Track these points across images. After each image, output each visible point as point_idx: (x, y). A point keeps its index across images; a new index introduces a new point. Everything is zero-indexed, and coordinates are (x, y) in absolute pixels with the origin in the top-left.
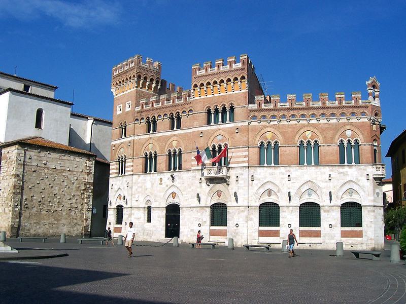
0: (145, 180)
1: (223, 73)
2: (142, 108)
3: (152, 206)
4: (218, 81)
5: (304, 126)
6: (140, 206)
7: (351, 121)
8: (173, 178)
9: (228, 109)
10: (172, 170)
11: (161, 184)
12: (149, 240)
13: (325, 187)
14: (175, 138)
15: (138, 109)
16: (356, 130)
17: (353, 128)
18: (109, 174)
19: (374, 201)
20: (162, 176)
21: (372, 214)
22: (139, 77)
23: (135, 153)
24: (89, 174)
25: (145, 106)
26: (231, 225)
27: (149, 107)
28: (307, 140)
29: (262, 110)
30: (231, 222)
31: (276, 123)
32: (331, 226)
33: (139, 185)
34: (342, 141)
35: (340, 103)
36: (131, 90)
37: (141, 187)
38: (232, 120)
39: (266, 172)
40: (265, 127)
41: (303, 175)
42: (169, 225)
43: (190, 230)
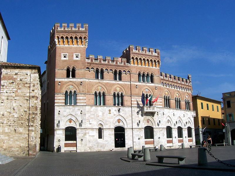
0: (97, 110)
1: (148, 55)
6: (94, 128)
8: (119, 111)
11: (110, 113)
12: (102, 150)
14: (118, 86)
18: (54, 103)
20: (110, 108)
27: (98, 62)
33: (92, 113)
37: (94, 115)
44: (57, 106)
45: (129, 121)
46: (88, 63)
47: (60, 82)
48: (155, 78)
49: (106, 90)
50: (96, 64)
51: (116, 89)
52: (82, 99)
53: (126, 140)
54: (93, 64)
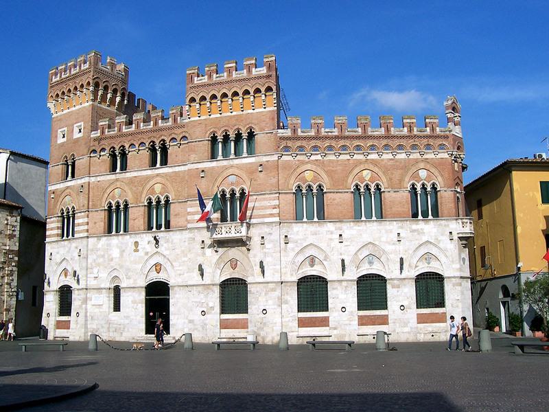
0: (109, 245)
2: (103, 132)
3: (122, 285)
4: (219, 96)
5: (359, 162)
6: (102, 286)
7: (425, 157)
9: (245, 135)
10: (154, 229)
11: (136, 251)
12: (118, 339)
13: (393, 251)
14: (158, 179)
15: (98, 134)
16: (433, 170)
17: (428, 167)
18: (44, 237)
19: (461, 270)
20: (138, 238)
21: (459, 288)
22: (97, 85)
23: (90, 203)
24: (11, 237)
25: (107, 130)
26: (255, 312)
27: (115, 132)
28: (364, 184)
29: (299, 138)
30: (254, 307)
31: (319, 157)
32: (402, 308)
34: (413, 185)
35: (410, 130)
36: (83, 105)
38: (251, 152)
39: (306, 230)
40: (303, 163)
41: (361, 235)
42: (151, 314)
43: (187, 321)
44: (48, 242)
45: (181, 268)
48: (260, 138)
51: (153, 189)
53: (171, 317)
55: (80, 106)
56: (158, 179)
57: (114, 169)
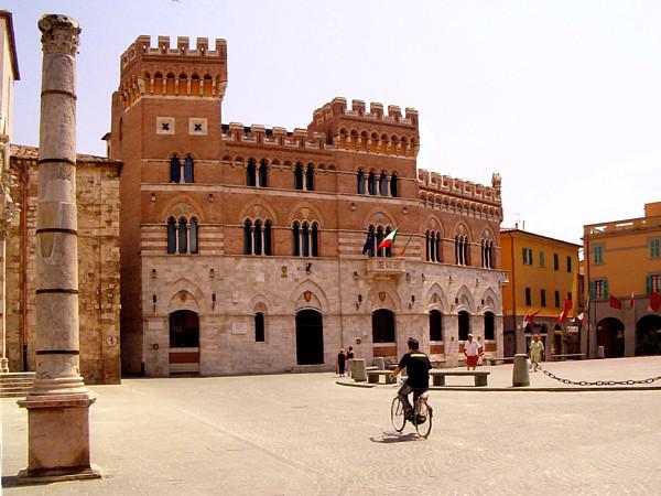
0: (251, 268)
6: (244, 312)
8: (308, 269)
11: (283, 276)
14: (306, 204)
33: (238, 275)
37: (244, 279)
46: (228, 144)
47: (153, 195)
49: (275, 217)
50: (249, 146)
52: (214, 240)
54: (242, 146)
55: (198, 98)
56: (306, 204)
57: (252, 183)
